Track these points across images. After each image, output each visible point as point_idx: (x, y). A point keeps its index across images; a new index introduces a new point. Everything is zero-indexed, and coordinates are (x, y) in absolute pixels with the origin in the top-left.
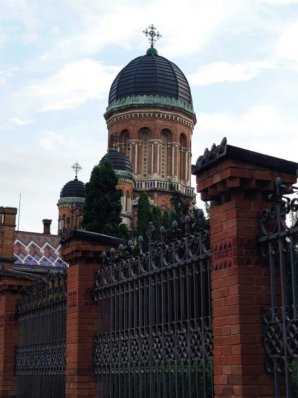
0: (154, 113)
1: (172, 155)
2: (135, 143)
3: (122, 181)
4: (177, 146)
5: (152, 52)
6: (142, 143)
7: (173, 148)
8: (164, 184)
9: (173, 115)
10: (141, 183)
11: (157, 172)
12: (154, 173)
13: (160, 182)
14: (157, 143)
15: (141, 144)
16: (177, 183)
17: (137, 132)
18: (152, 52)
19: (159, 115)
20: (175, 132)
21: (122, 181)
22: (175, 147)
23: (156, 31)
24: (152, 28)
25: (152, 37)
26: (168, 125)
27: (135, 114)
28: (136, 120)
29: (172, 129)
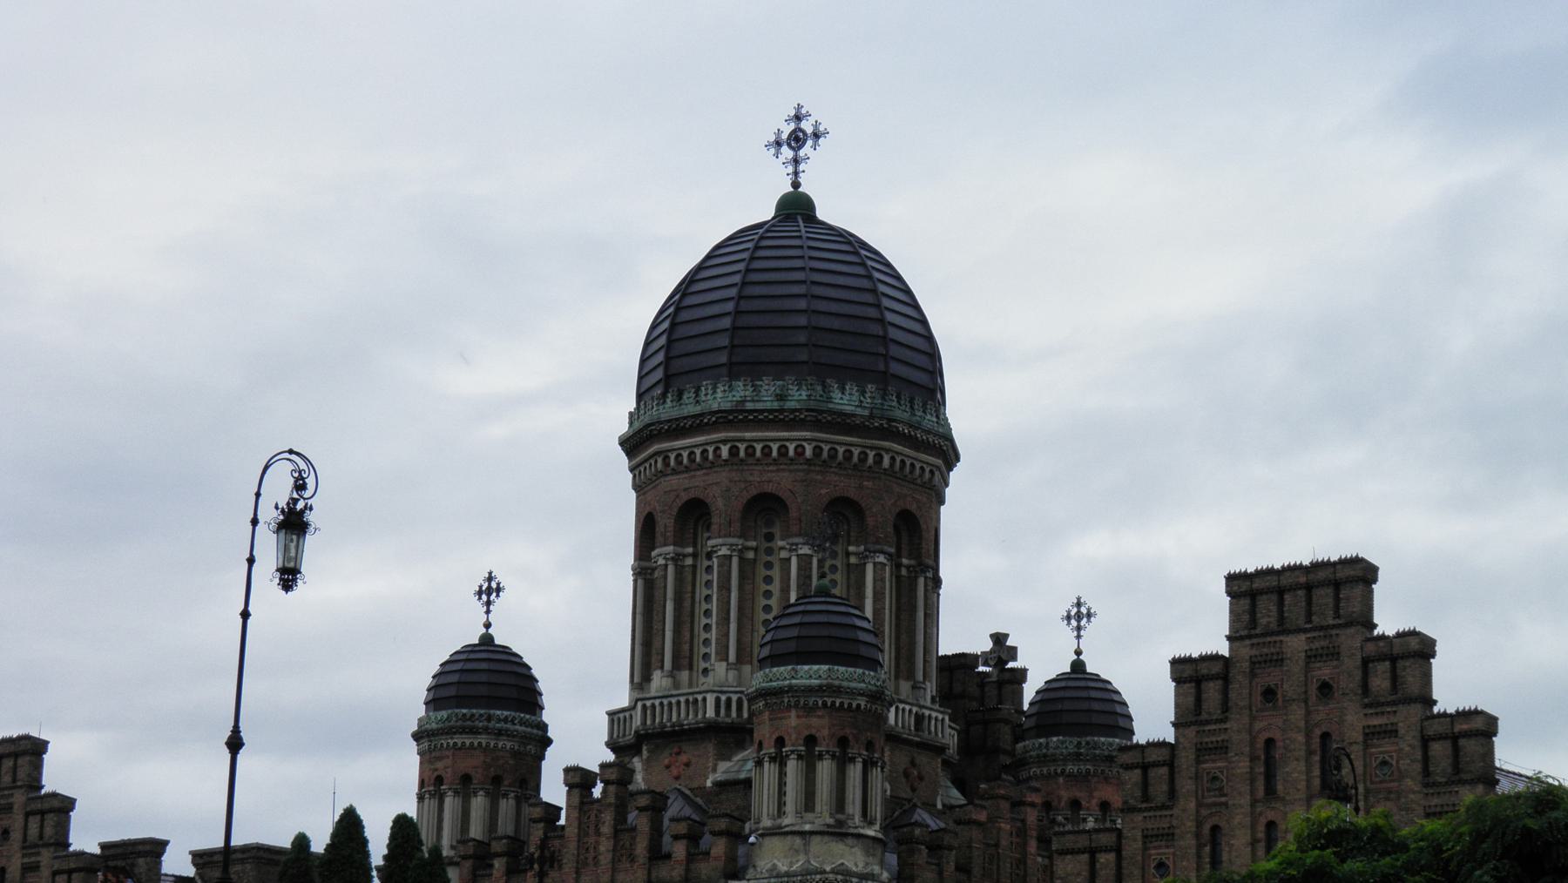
4: (724, 551)
5: (796, 208)
8: (661, 704)
11: (662, 668)
13: (648, 703)
18: (796, 208)
20: (720, 503)
23: (807, 126)
24: (798, 118)
25: (796, 150)
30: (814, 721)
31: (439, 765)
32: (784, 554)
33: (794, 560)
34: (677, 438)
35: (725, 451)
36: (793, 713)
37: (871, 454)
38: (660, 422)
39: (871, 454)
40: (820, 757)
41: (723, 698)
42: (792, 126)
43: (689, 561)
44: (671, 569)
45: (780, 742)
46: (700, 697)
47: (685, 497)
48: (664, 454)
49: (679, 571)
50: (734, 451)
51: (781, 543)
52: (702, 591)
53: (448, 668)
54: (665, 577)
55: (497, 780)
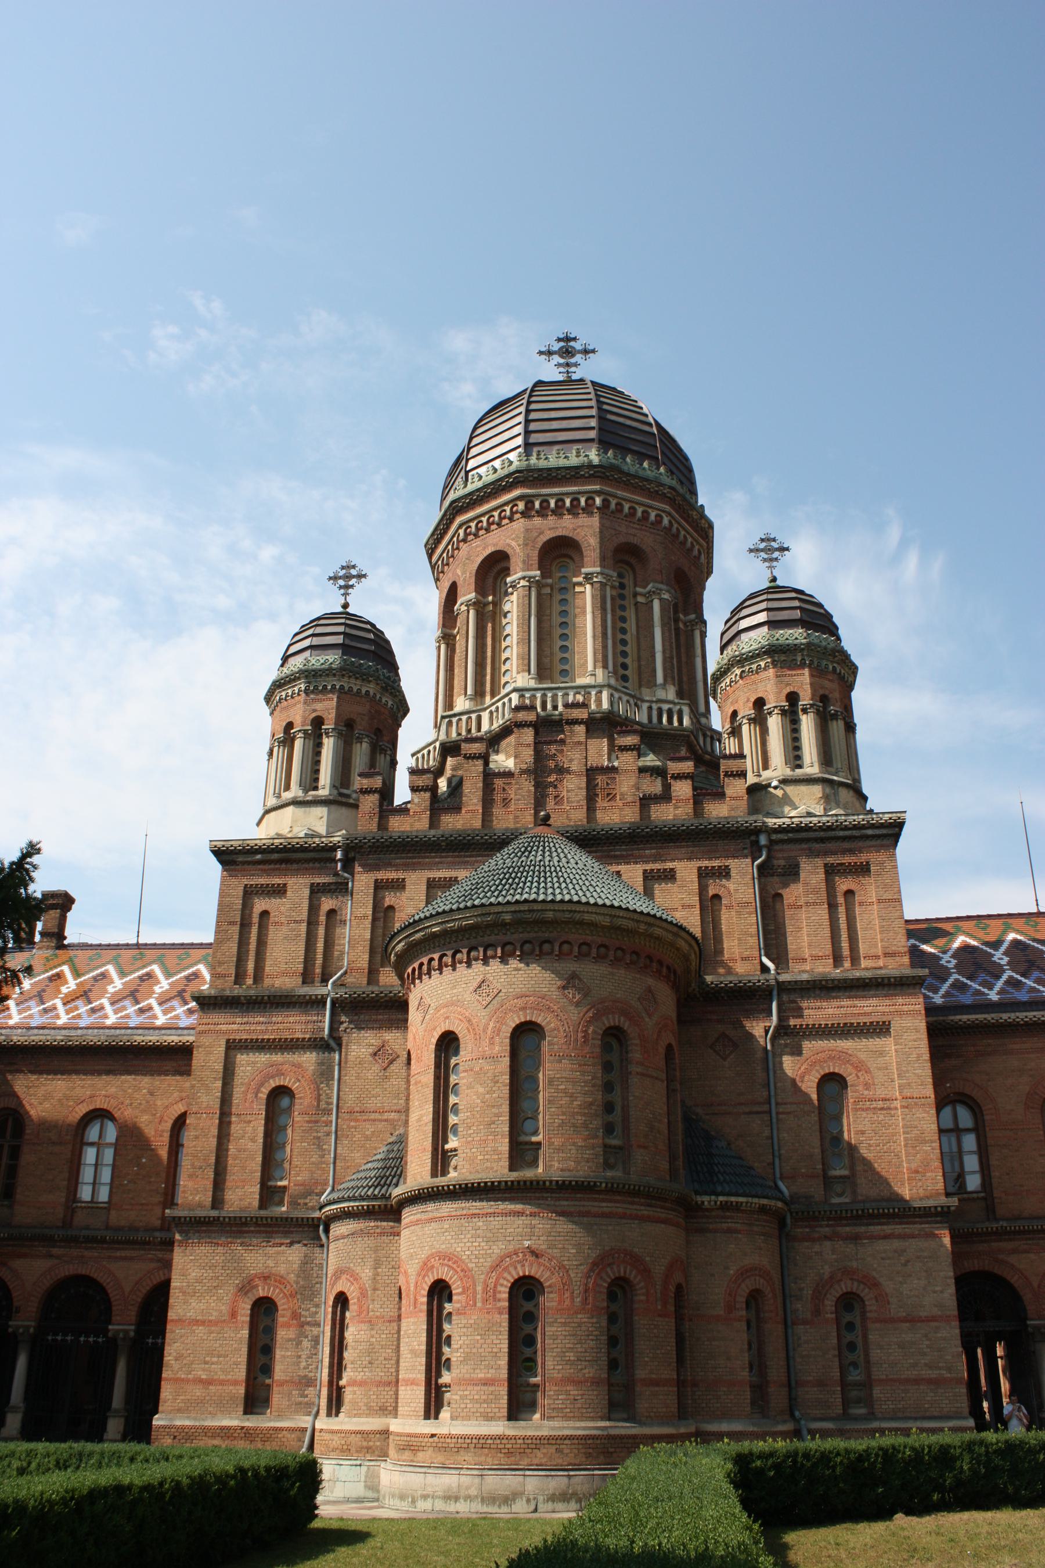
0: (513, 502)
8: (544, 696)
17: (474, 572)
29: (578, 536)
30: (827, 684)
31: (319, 706)
32: (640, 599)
33: (656, 604)
34: (543, 486)
36: (806, 671)
37: (697, 547)
39: (697, 547)
40: (834, 717)
47: (549, 535)
48: (529, 500)
50: (606, 503)
51: (639, 589)
52: (557, 620)
55: (378, 732)
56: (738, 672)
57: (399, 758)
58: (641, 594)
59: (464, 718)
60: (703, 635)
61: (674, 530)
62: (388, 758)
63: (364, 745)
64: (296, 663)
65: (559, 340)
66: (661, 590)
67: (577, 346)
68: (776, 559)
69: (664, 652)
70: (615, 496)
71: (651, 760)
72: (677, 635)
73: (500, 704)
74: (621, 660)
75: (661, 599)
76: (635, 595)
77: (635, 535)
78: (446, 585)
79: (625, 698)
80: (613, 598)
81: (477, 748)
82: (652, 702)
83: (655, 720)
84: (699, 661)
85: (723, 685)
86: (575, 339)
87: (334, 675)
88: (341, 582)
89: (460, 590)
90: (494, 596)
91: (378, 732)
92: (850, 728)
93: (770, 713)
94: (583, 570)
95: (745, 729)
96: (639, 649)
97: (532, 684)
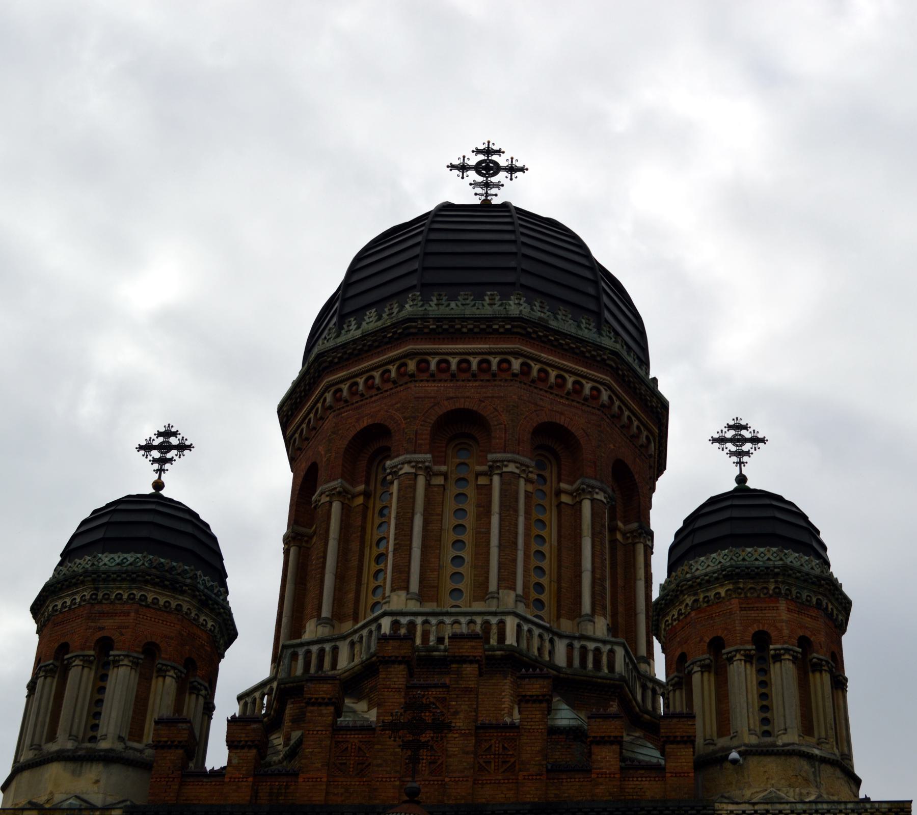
1: (488, 513)
2: (328, 499)
3: (119, 597)
4: (511, 468)
6: (367, 495)
7: (496, 479)
8: (426, 622)
9: (490, 353)
10: (335, 650)
11: (407, 588)
12: (393, 594)
14: (413, 471)
15: (360, 500)
16: (495, 614)
19: (423, 366)
21: (119, 597)
22: (501, 475)
24: (488, 151)
26: (469, 395)
27: (333, 389)
28: (337, 412)
32: (565, 498)
33: (587, 506)
35: (516, 364)
36: (783, 605)
38: (424, 319)
41: (525, 627)
42: (481, 157)
43: (439, 481)
44: (421, 481)
45: (761, 639)
46: (494, 620)
47: (448, 406)
49: (428, 485)
51: (563, 486)
52: (450, 520)
53: (82, 529)
54: (414, 488)
56: (689, 600)
57: (216, 701)
58: (566, 492)
59: (315, 649)
60: (649, 550)
61: (615, 408)
62: (201, 700)
63: (168, 680)
64: (84, 563)
65: (478, 152)
66: (593, 487)
67: (502, 161)
68: (748, 453)
69: (593, 572)
70: (537, 360)
71: (565, 716)
72: (613, 550)
73: (365, 632)
74: (534, 579)
75: (593, 501)
76: (559, 493)
77: (562, 414)
78: (304, 466)
79: (536, 631)
80: (528, 495)
81: (324, 690)
82: (574, 638)
83: (576, 662)
84: (641, 584)
85: (669, 618)
86: (499, 152)
87: (133, 581)
88: (156, 454)
89: (322, 474)
90: (367, 483)
91: (190, 664)
92: (840, 684)
93: (730, 660)
94: (490, 457)
95: (696, 678)
96: (559, 567)
97: (413, 606)
